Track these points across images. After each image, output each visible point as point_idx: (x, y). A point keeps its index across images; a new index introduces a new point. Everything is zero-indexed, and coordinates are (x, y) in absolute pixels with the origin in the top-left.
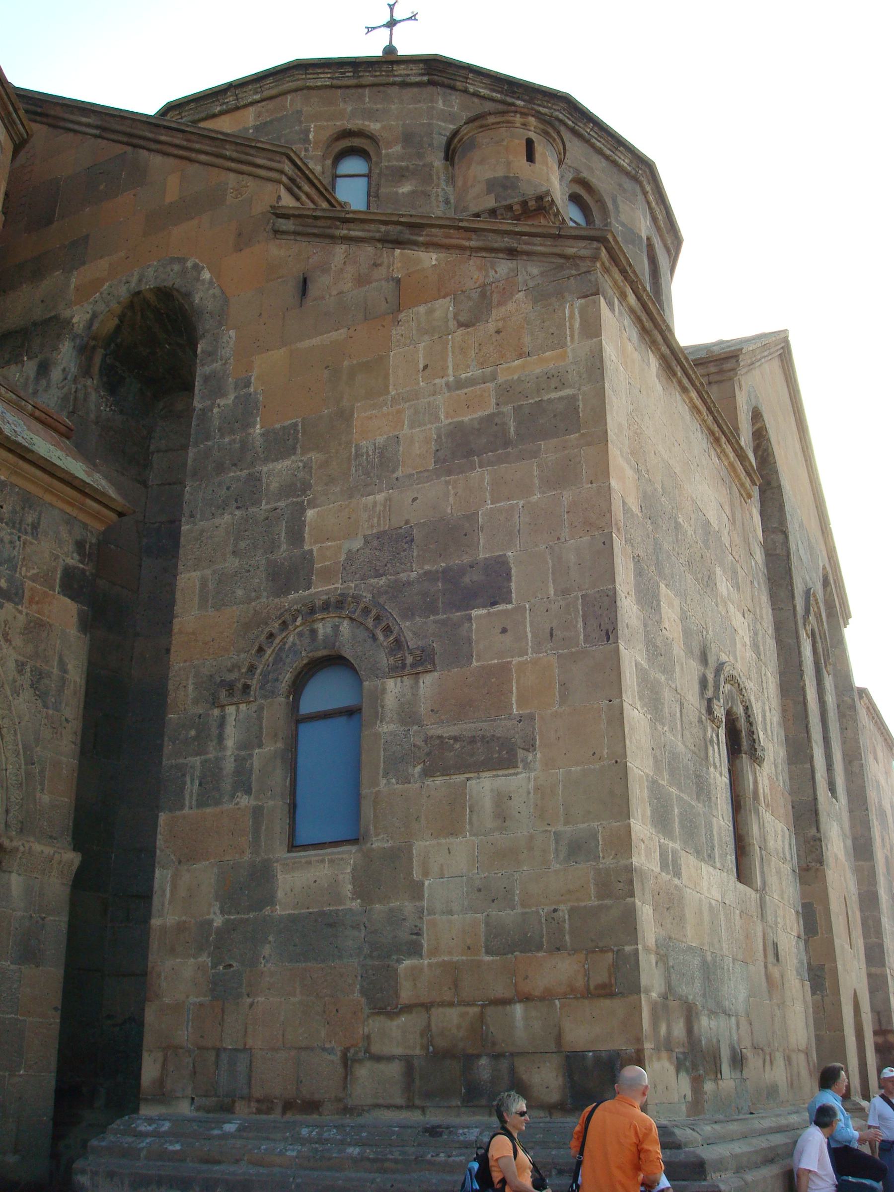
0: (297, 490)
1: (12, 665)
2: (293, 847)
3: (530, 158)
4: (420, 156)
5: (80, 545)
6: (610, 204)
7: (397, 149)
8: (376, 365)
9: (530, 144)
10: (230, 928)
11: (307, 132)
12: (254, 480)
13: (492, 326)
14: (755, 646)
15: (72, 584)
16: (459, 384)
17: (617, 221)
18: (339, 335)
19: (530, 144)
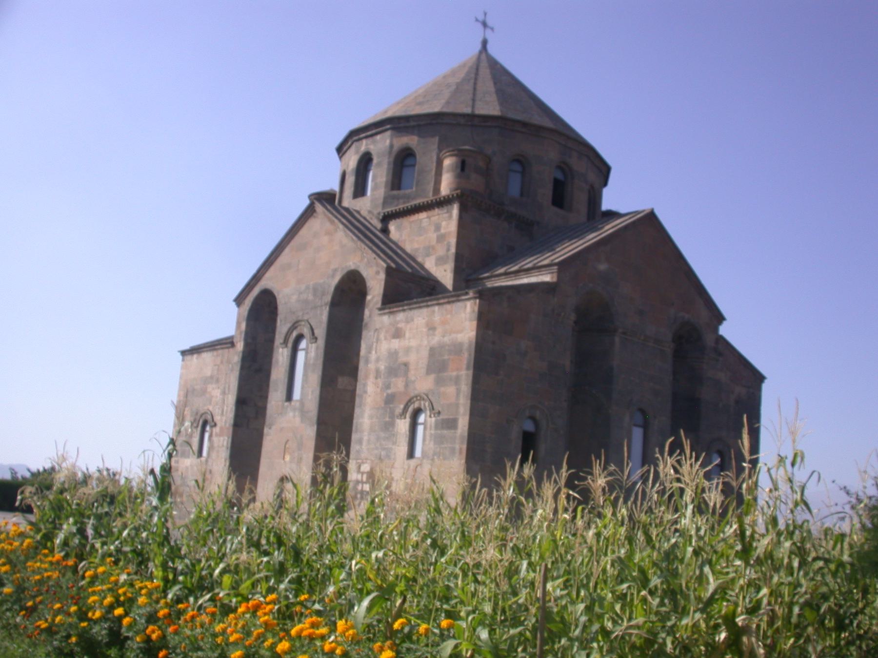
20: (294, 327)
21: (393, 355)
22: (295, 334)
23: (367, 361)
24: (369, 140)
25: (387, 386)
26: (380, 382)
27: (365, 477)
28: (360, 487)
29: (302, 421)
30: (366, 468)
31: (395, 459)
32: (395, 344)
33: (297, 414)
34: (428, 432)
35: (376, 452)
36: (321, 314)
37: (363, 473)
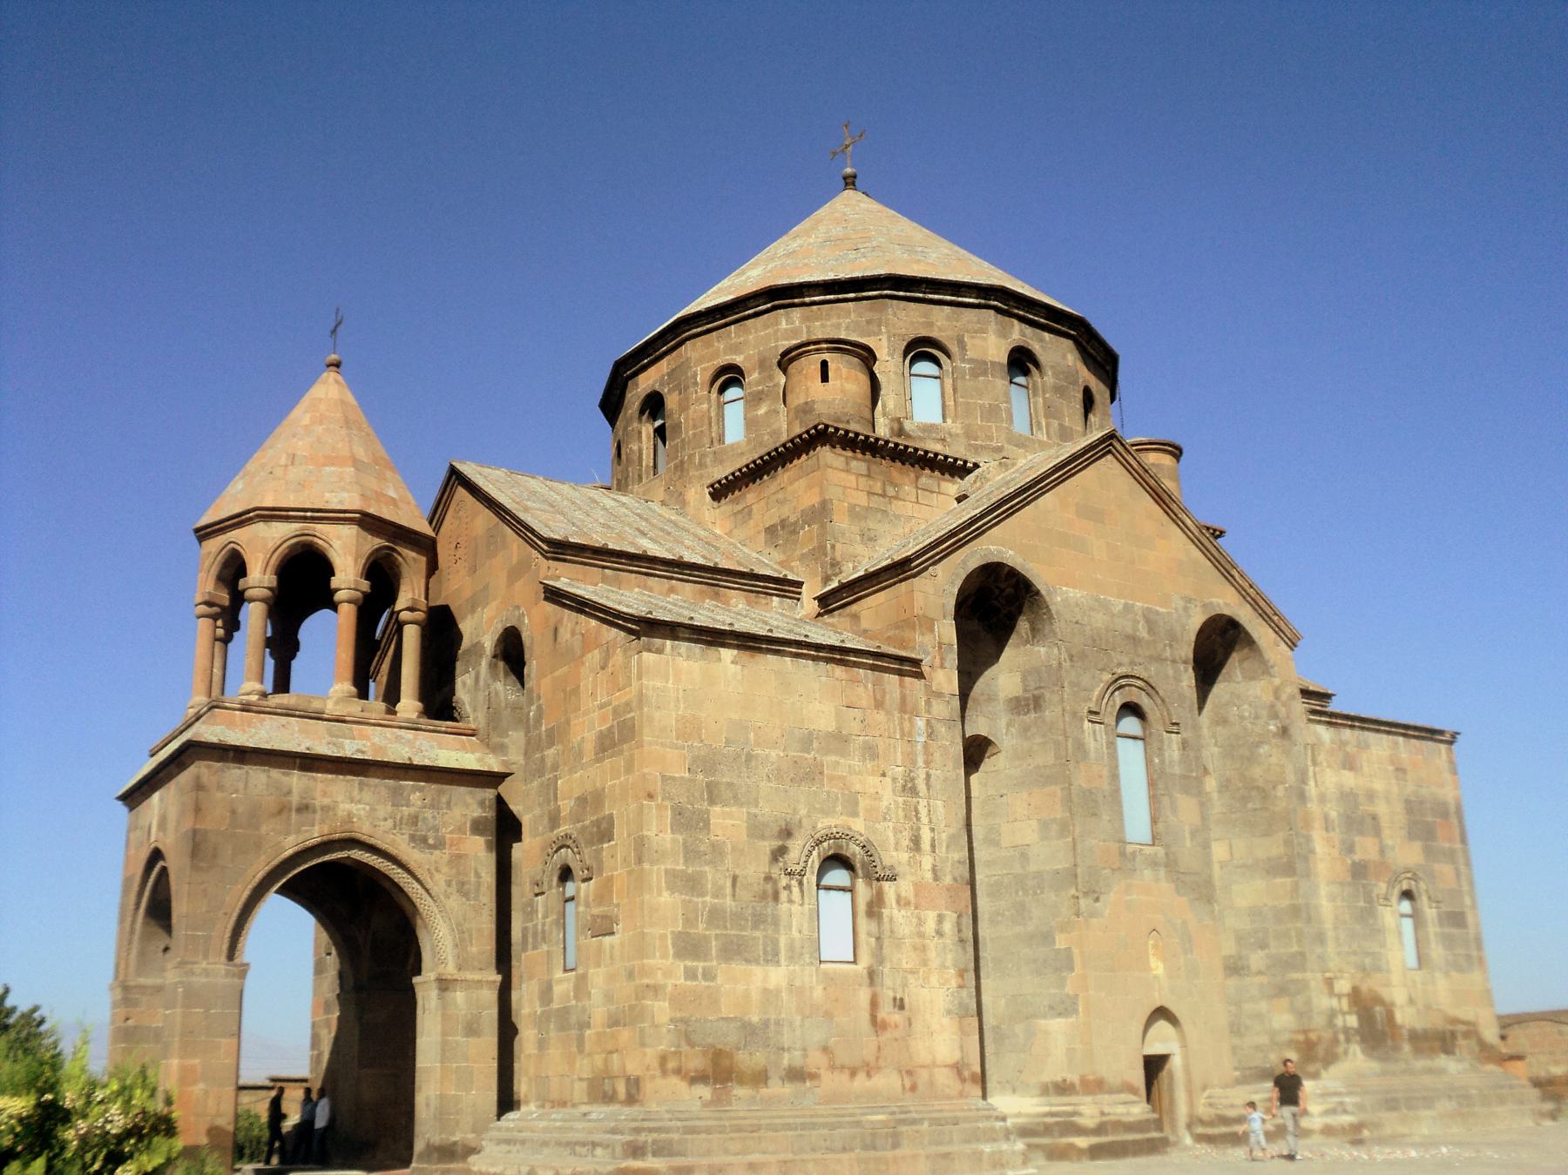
0: (555, 767)
1: (443, 883)
2: (565, 971)
3: (825, 378)
4: (771, 378)
5: (482, 803)
6: (953, 348)
7: (756, 375)
8: (576, 690)
9: (824, 364)
10: (543, 1013)
11: (695, 375)
12: (543, 759)
13: (610, 670)
14: (909, 788)
15: (477, 827)
16: (602, 706)
17: (963, 360)
18: (565, 669)
19: (824, 364)
20: (1118, 683)
21: (1348, 797)
22: (1119, 699)
23: (1302, 797)
24: (1029, 330)
25: (1350, 849)
26: (1336, 836)
27: (1345, 1004)
28: (1339, 1021)
29: (1177, 890)
30: (1343, 986)
31: (1389, 971)
32: (1349, 779)
33: (1162, 872)
34: (1433, 929)
35: (1353, 959)
36: (1178, 679)
37: (1339, 996)
